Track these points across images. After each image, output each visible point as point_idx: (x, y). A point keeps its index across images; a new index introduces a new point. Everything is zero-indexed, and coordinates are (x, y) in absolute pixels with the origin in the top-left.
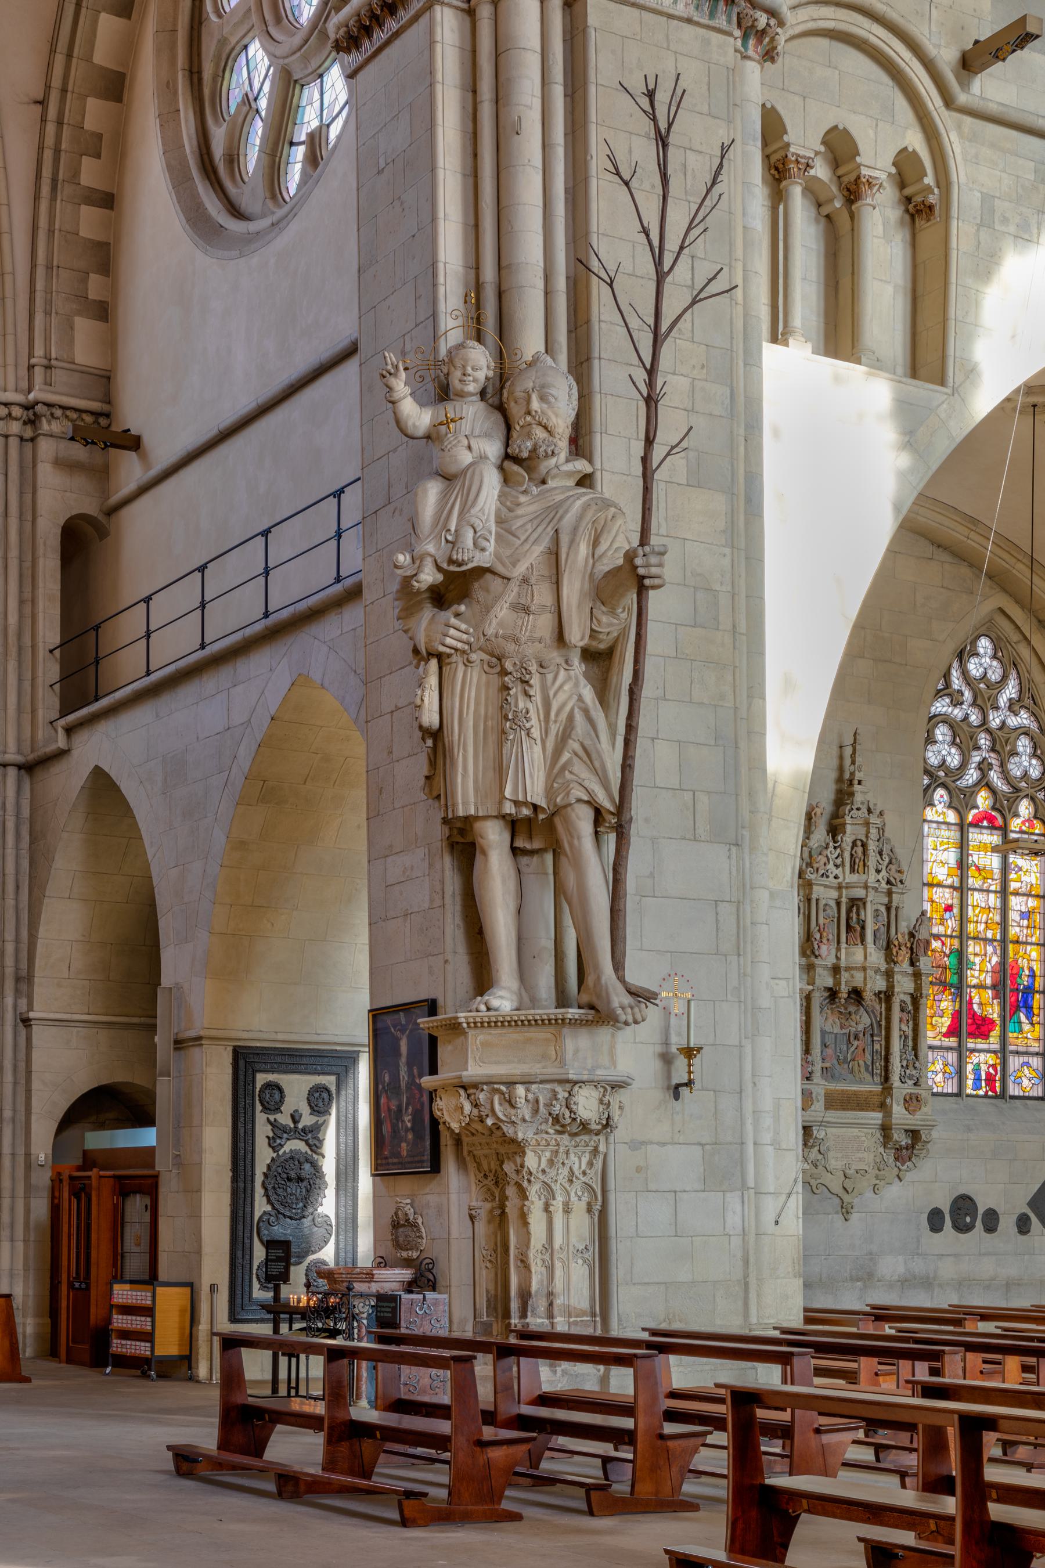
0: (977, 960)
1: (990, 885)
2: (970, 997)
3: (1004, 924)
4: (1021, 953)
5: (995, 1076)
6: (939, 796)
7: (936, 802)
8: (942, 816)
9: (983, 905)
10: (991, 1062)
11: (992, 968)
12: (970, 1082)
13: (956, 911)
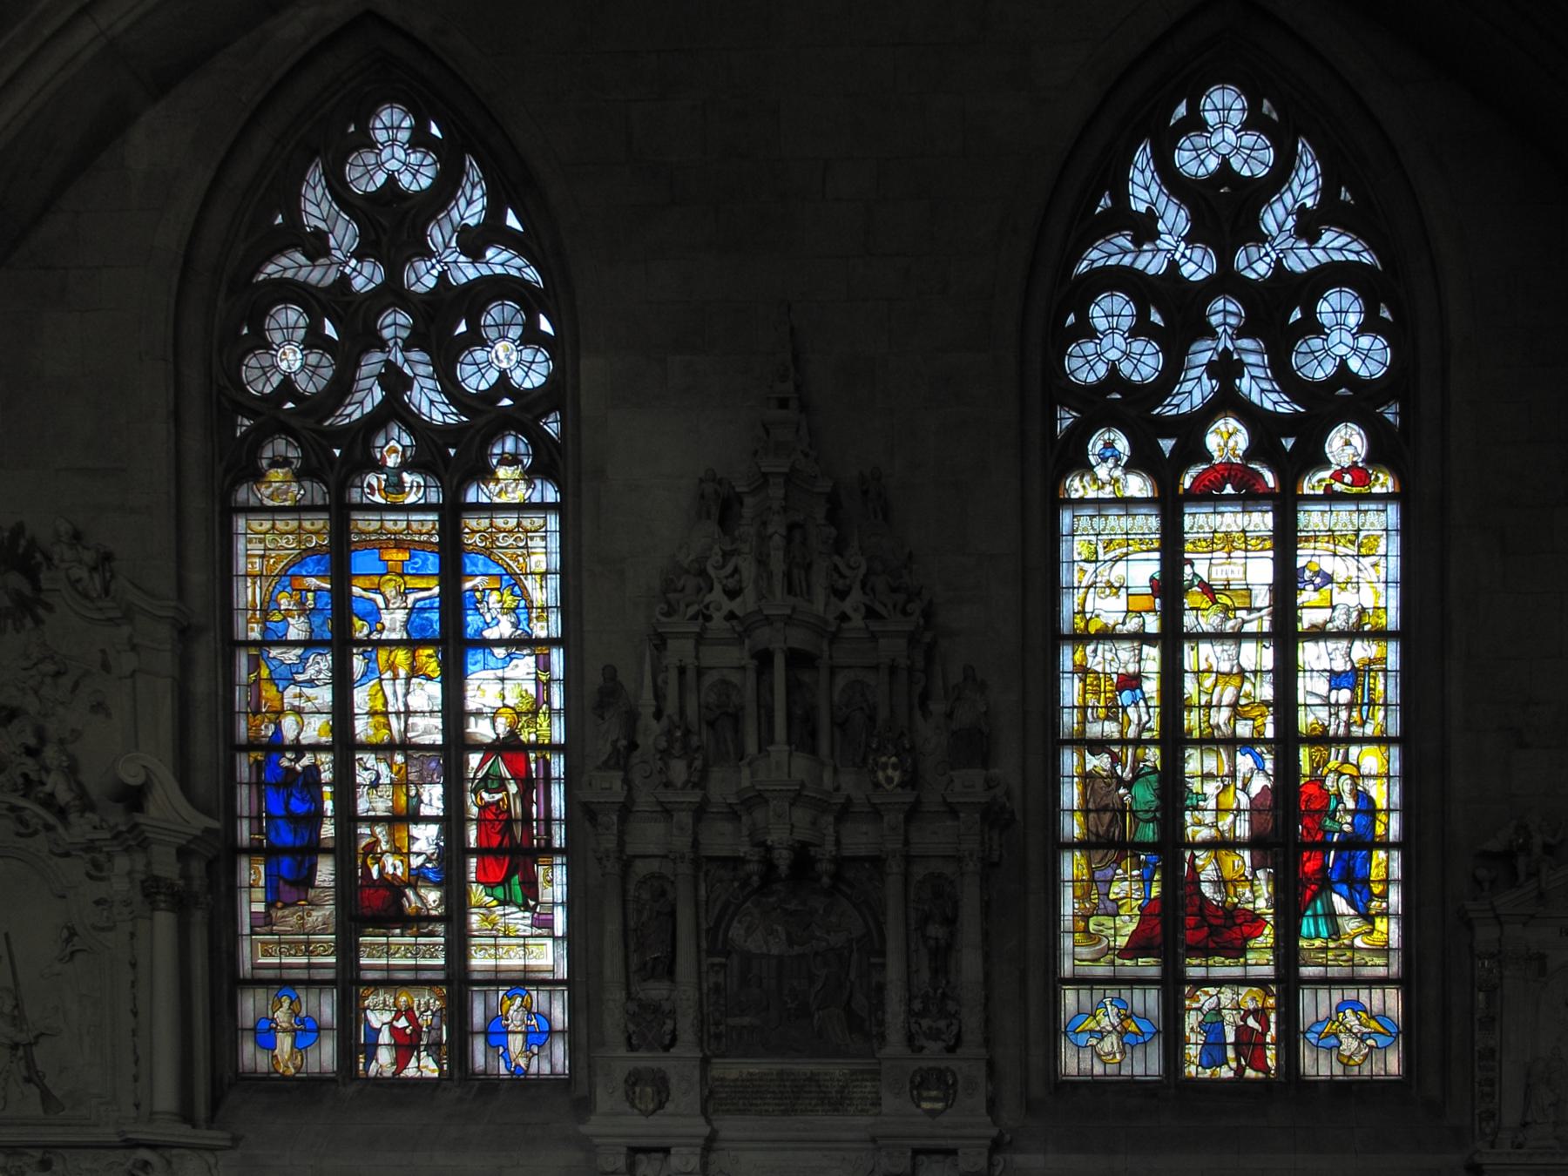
0: (1211, 788)
1: (1244, 622)
2: (1193, 867)
3: (1285, 703)
4: (1333, 764)
5: (1264, 1034)
6: (1100, 445)
7: (1093, 460)
8: (1109, 489)
9: (1225, 667)
10: (1251, 1006)
11: (1252, 801)
13: (1151, 687)
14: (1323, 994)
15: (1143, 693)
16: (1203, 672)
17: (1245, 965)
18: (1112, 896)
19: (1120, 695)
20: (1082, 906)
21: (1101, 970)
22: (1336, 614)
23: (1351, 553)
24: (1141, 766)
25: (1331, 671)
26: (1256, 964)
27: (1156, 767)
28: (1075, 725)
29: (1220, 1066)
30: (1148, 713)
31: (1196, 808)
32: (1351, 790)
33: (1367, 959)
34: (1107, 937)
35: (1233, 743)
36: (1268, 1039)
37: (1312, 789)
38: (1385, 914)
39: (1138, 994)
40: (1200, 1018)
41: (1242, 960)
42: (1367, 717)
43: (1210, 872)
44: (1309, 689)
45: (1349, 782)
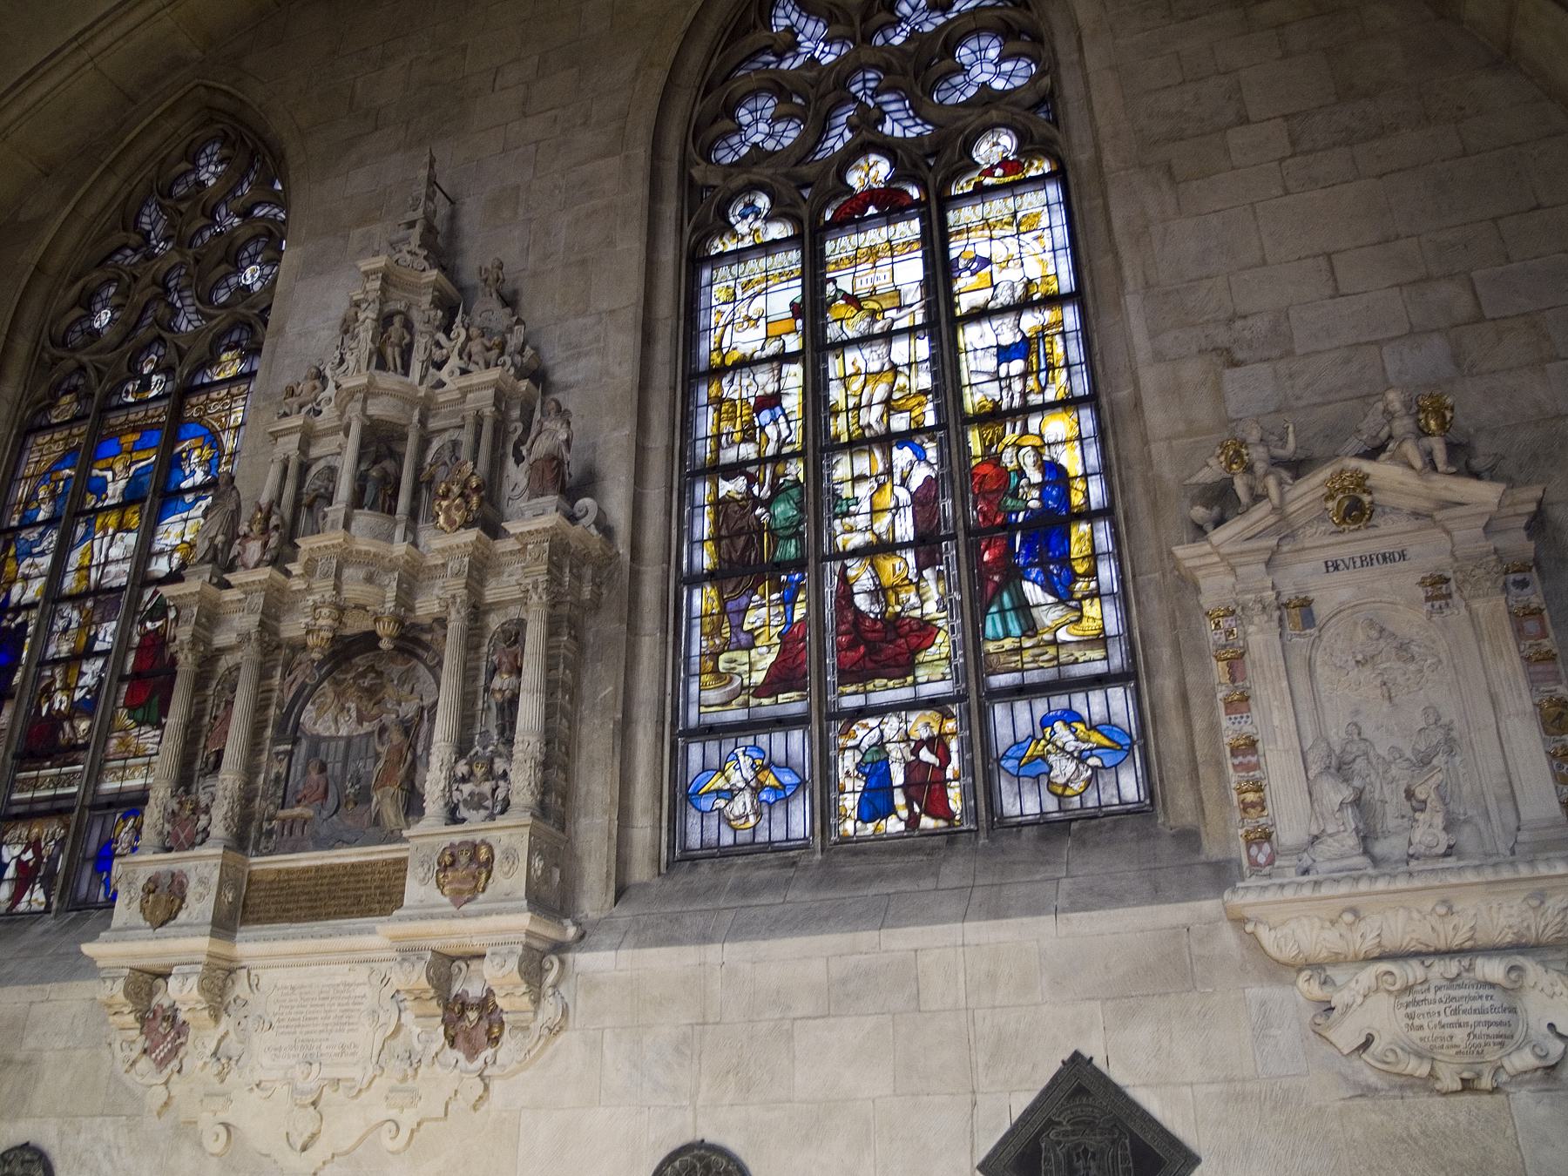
0: (863, 490)
1: (893, 321)
4: (1010, 438)
5: (943, 767)
11: (913, 495)
12: (850, 802)
13: (792, 402)
14: (1021, 707)
15: (783, 410)
16: (850, 376)
17: (915, 684)
18: (746, 627)
19: (758, 416)
20: (711, 643)
21: (735, 714)
22: (999, 290)
23: (1008, 233)
24: (781, 481)
25: (998, 346)
26: (928, 682)
27: (798, 479)
28: (708, 455)
29: (886, 817)
30: (789, 427)
31: (847, 514)
32: (1035, 463)
33: (1077, 654)
34: (740, 675)
35: (888, 440)
36: (949, 774)
37: (988, 469)
38: (1095, 594)
39: (778, 738)
40: (858, 758)
41: (910, 679)
42: (1047, 382)
43: (866, 582)
44: (972, 368)
45: (1032, 453)
